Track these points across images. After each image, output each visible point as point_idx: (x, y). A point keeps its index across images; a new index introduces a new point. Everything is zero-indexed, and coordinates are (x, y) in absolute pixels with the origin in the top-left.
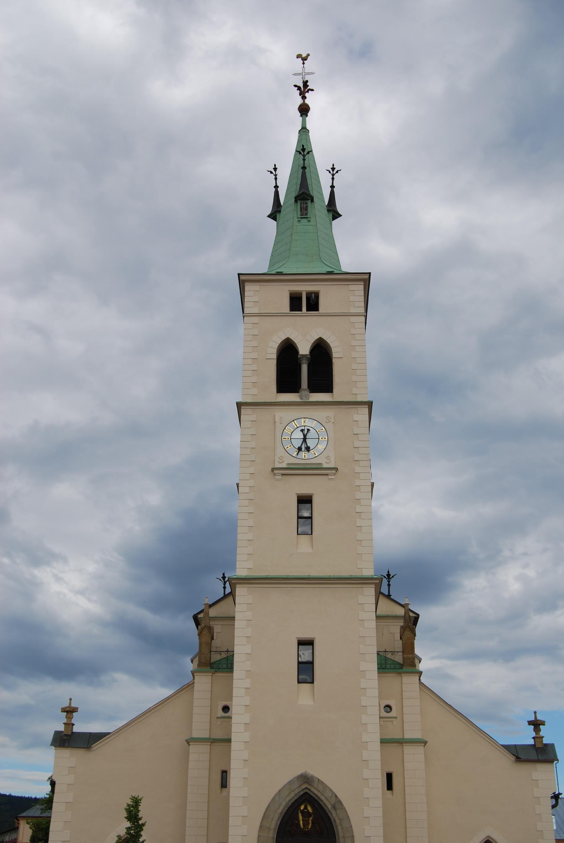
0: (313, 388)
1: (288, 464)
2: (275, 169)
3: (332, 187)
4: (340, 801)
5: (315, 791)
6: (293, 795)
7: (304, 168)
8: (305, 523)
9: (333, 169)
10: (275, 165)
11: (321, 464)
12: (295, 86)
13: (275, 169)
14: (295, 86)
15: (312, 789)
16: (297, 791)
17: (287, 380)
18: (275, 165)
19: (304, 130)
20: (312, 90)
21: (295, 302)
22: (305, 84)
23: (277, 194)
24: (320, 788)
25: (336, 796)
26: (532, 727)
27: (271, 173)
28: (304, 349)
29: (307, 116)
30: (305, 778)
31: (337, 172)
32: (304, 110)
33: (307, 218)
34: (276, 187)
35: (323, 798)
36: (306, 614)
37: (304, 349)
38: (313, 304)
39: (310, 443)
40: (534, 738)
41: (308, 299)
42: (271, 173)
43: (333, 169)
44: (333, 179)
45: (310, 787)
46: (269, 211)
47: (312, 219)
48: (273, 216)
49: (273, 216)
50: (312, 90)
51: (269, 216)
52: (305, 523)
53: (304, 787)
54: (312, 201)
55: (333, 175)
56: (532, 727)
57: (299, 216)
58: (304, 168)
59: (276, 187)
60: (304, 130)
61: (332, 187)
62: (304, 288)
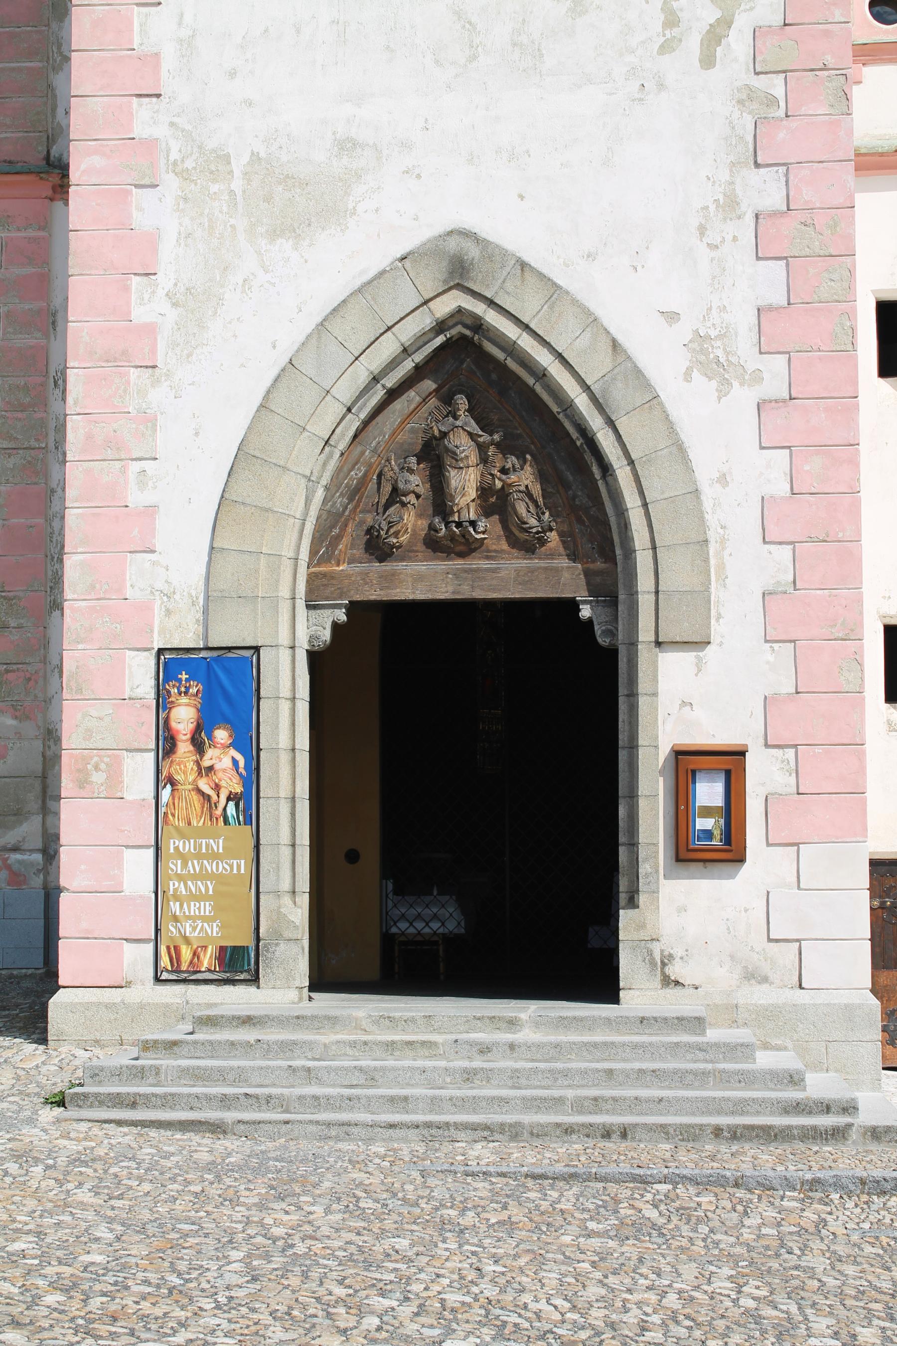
4: (638, 372)
6: (388, 348)
15: (492, 318)
16: (409, 330)
30: (458, 262)
53: (444, 307)
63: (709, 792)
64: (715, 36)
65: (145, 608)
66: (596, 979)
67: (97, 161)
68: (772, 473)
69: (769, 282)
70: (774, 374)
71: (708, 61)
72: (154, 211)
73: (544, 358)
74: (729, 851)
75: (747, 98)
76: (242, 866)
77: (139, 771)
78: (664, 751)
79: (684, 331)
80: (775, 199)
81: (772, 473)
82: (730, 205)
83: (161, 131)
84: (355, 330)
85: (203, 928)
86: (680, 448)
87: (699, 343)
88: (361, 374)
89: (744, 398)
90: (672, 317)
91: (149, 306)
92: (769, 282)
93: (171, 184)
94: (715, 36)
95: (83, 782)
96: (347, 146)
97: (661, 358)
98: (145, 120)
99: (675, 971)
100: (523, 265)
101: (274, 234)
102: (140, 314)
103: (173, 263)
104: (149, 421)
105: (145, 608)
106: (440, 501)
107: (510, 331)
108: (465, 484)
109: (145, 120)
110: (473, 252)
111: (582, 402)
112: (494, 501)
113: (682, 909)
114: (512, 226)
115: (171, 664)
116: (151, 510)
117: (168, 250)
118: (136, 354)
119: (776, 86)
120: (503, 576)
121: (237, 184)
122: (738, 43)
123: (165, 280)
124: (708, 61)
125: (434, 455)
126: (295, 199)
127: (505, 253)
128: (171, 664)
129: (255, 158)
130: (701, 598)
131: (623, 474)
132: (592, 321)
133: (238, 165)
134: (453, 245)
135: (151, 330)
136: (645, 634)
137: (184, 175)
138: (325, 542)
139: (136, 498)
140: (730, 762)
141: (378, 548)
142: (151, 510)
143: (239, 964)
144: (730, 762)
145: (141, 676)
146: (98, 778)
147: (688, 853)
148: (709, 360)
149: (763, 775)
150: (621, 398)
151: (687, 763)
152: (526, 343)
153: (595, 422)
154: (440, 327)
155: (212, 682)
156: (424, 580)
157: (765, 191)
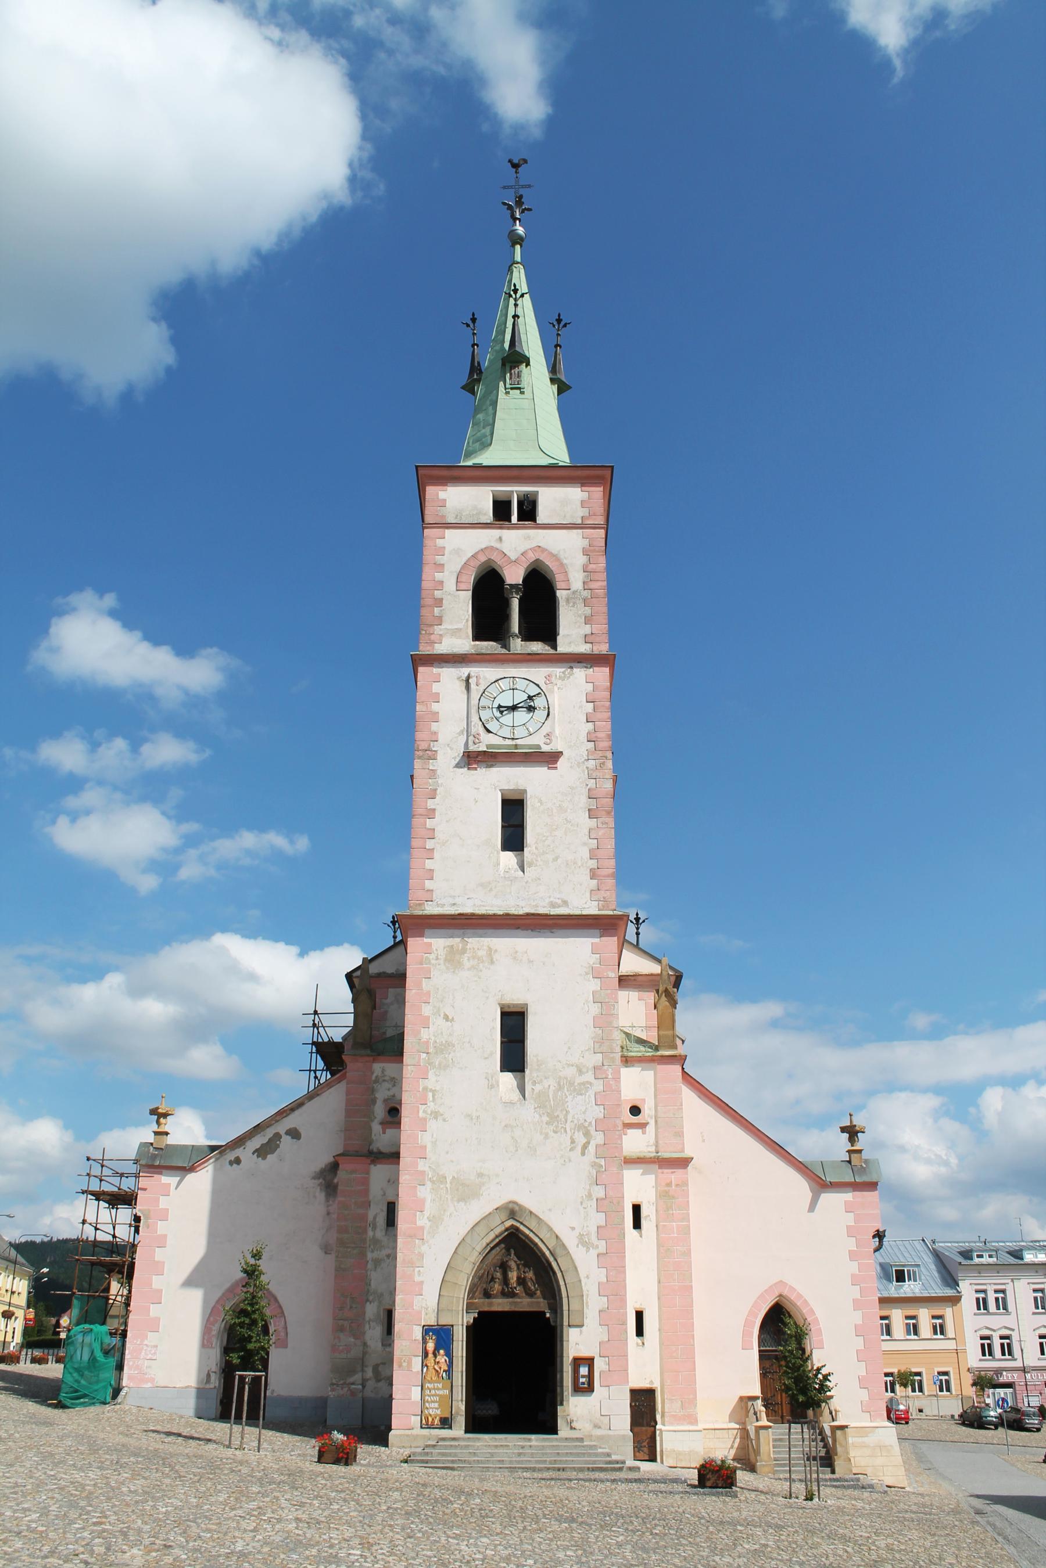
0: (528, 636)
1: (488, 746)
2: (474, 320)
4: (564, 1245)
5: (529, 1229)
6: (492, 1236)
8: (513, 836)
9: (559, 321)
10: (473, 314)
13: (474, 320)
15: (522, 1227)
16: (498, 1231)
17: (488, 621)
18: (473, 314)
20: (529, 210)
21: (501, 510)
24: (533, 1225)
25: (557, 1237)
26: (846, 1135)
27: (468, 325)
28: (514, 576)
30: (512, 1211)
31: (565, 325)
33: (519, 388)
36: (515, 969)
37: (514, 576)
38: (528, 511)
39: (520, 697)
40: (848, 1151)
41: (520, 504)
42: (468, 325)
43: (559, 321)
45: (518, 1225)
51: (463, 388)
52: (513, 836)
53: (508, 1224)
54: (528, 364)
56: (846, 1135)
63: (584, 1370)
64: (585, 1147)
65: (420, 1312)
66: (551, 1428)
67: (407, 1177)
68: (601, 1275)
69: (600, 1219)
70: (602, 1246)
71: (583, 1154)
72: (425, 1192)
73: (537, 1240)
74: (590, 1389)
75: (594, 1165)
76: (447, 1392)
77: (417, 1362)
78: (571, 1358)
79: (576, 1233)
80: (602, 1195)
81: (601, 1275)
82: (589, 1196)
83: (426, 1169)
84: (482, 1230)
85: (435, 1411)
86: (576, 1268)
87: (581, 1236)
89: (594, 1253)
90: (573, 1229)
91: (422, 1221)
92: (600, 1219)
93: (429, 1184)
94: (585, 1147)
95: (400, 1366)
96: (480, 1175)
97: (570, 1241)
98: (422, 1166)
99: (574, 1425)
100: (531, 1212)
101: (459, 1201)
102: (419, 1223)
103: (429, 1208)
104: (421, 1256)
106: (506, 1281)
108: (513, 1276)
109: (422, 1166)
110: (517, 1208)
111: (547, 1253)
112: (521, 1281)
114: (527, 1201)
115: (427, 1330)
116: (422, 1282)
117: (428, 1204)
118: (418, 1234)
119: (602, 1162)
120: (524, 1304)
121: (448, 1185)
122: (591, 1149)
123: (427, 1213)
124: (583, 1154)
125: (504, 1267)
126: (465, 1190)
127: (525, 1209)
128: (427, 1330)
129: (454, 1177)
130: (581, 1313)
131: (559, 1275)
132: (551, 1229)
134: (511, 1205)
135: (422, 1228)
136: (565, 1323)
137: (433, 1182)
138: (472, 1292)
139: (417, 1279)
140: (590, 1362)
141: (487, 1295)
142: (422, 1282)
143: (446, 1423)
144: (590, 1362)
145: (418, 1333)
146: (405, 1364)
147: (578, 1389)
148: (583, 1241)
149: (599, 1365)
150: (559, 1252)
151: (577, 1362)
152: (531, 1235)
153: (551, 1259)
154: (507, 1230)
155: (441, 1335)
156: (500, 1305)
157: (599, 1192)
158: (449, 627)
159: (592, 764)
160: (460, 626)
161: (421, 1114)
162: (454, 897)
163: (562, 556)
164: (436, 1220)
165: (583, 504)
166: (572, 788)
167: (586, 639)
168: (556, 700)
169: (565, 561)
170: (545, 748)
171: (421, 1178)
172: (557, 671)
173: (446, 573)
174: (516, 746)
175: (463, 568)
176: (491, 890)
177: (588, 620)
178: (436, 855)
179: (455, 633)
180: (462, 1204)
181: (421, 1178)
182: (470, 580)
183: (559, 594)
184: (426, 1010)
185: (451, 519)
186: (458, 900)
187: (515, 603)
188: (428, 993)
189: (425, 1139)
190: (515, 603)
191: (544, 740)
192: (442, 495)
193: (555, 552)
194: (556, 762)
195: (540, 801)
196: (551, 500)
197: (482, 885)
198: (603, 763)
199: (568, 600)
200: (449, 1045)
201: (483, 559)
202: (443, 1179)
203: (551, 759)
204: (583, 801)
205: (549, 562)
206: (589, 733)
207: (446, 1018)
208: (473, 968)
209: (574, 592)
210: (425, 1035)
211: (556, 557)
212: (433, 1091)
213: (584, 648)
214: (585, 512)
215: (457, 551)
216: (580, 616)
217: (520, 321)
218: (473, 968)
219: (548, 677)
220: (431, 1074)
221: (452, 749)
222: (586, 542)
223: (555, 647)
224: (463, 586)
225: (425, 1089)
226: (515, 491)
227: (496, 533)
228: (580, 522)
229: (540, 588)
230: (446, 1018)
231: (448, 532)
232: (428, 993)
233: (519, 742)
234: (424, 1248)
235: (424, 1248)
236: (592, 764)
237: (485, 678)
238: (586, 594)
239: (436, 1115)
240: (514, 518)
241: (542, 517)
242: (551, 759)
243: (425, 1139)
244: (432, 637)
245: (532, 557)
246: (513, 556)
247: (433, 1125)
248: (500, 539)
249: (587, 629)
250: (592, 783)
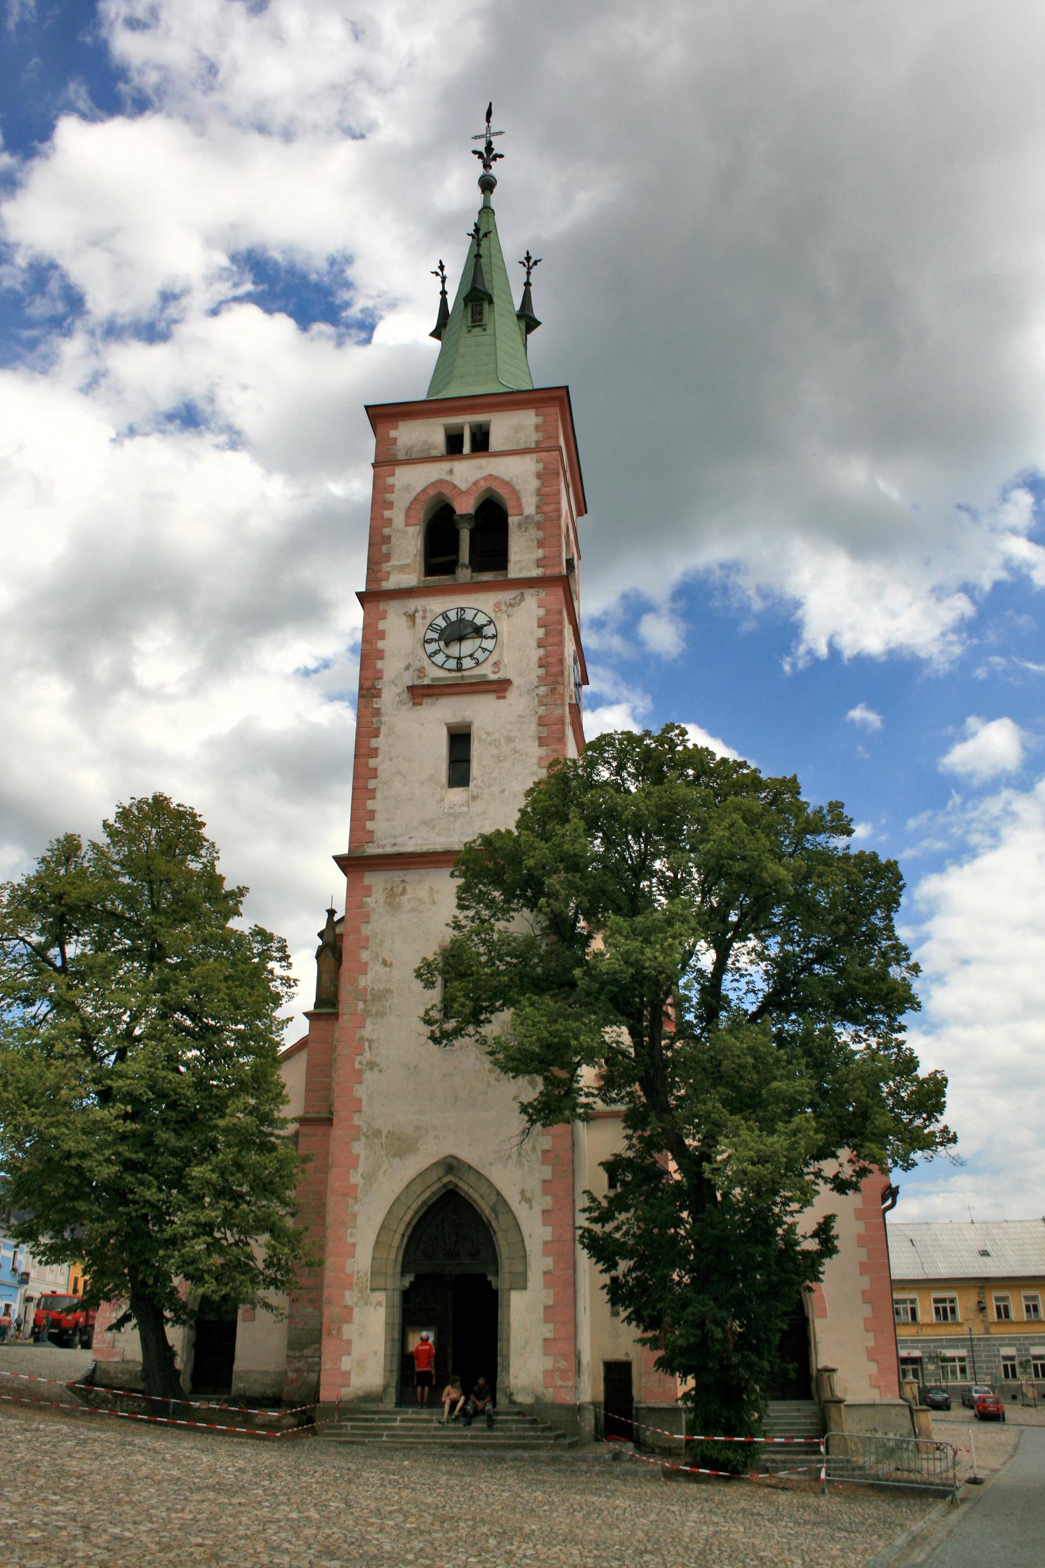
0: (479, 564)
1: (433, 679)
2: (442, 267)
3: (528, 284)
4: (505, 1202)
6: (428, 1193)
7: (478, 256)
8: (459, 769)
9: (528, 259)
11: (485, 675)
12: (475, 152)
13: (442, 267)
14: (475, 152)
15: (461, 1184)
16: (434, 1188)
19: (486, 210)
20: (501, 156)
22: (489, 147)
23: (444, 303)
24: (472, 1178)
28: (465, 506)
29: (492, 192)
30: (451, 1165)
31: (535, 263)
32: (487, 185)
34: (444, 293)
35: (476, 1196)
37: (465, 506)
38: (481, 442)
41: (473, 435)
42: (437, 274)
43: (528, 259)
44: (528, 273)
46: (432, 325)
47: (490, 328)
48: (436, 334)
49: (436, 334)
50: (501, 156)
53: (445, 1180)
54: (491, 302)
55: (529, 268)
57: (470, 324)
58: (478, 256)
59: (444, 293)
60: (486, 210)
61: (528, 284)
62: (466, 421)
67: (341, 1132)
69: (547, 1172)
70: (547, 1202)
72: (359, 1148)
83: (361, 1123)
84: (418, 1188)
86: (518, 1226)
87: (523, 1192)
88: (420, 1201)
89: (538, 1209)
91: (356, 1179)
92: (547, 1172)
93: (363, 1138)
95: (330, 1333)
96: (417, 1128)
97: (513, 1199)
100: (470, 1167)
101: (395, 1156)
102: (353, 1181)
104: (354, 1216)
105: (351, 1276)
107: (466, 1188)
109: (357, 1120)
110: (455, 1163)
113: (516, 1377)
114: (467, 1155)
116: (354, 1245)
118: (350, 1192)
121: (383, 1140)
123: (360, 1170)
126: (401, 1145)
127: (465, 1163)
129: (389, 1132)
132: (491, 1185)
133: (384, 1133)
134: (449, 1160)
135: (356, 1186)
137: (367, 1137)
139: (350, 1240)
142: (354, 1245)
146: (334, 1332)
152: (471, 1192)
153: (492, 1217)
154: (445, 1186)
158: (397, 563)
159: (542, 690)
160: (408, 561)
161: (357, 1066)
162: (395, 837)
163: (515, 482)
164: (369, 1178)
165: (538, 428)
166: (521, 717)
167: (539, 563)
168: (504, 627)
169: (517, 487)
170: (493, 677)
171: (356, 1133)
172: (507, 596)
173: (395, 510)
174: (462, 677)
175: (412, 503)
176: (434, 827)
177: (541, 544)
178: (379, 795)
179: (403, 568)
180: (398, 1159)
181: (356, 1133)
182: (420, 515)
183: (513, 520)
184: (365, 956)
185: (401, 456)
186: (400, 840)
187: (465, 536)
188: (367, 938)
189: (361, 1091)
190: (465, 536)
191: (493, 669)
192: (393, 434)
193: (507, 479)
194: (505, 690)
195: (489, 734)
196: (503, 428)
197: (425, 823)
198: (555, 689)
199: (519, 526)
200: (389, 991)
201: (432, 492)
202: (377, 1134)
203: (500, 687)
204: (532, 728)
205: (503, 492)
206: (540, 659)
207: (385, 963)
208: (413, 910)
209: (527, 518)
210: (363, 982)
211: (507, 484)
212: (371, 1042)
213: (536, 572)
214: (540, 436)
215: (407, 488)
216: (532, 541)
217: (482, 260)
218: (413, 910)
219: (498, 605)
220: (368, 1021)
221: (396, 685)
222: (540, 466)
223: (506, 575)
224: (412, 521)
225: (362, 1038)
226: (466, 421)
227: (445, 466)
228: (533, 446)
229: (492, 516)
230: (385, 963)
231: (399, 471)
232: (367, 938)
233: (466, 673)
234: (357, 1208)
235: (357, 1208)
236: (542, 690)
237: (431, 611)
238: (538, 518)
239: (372, 1065)
240: (467, 448)
241: (496, 442)
242: (500, 687)
243: (361, 1091)
244: (380, 575)
245: (484, 485)
246: (463, 487)
247: (369, 1076)
248: (451, 472)
249: (540, 553)
250: (542, 710)
